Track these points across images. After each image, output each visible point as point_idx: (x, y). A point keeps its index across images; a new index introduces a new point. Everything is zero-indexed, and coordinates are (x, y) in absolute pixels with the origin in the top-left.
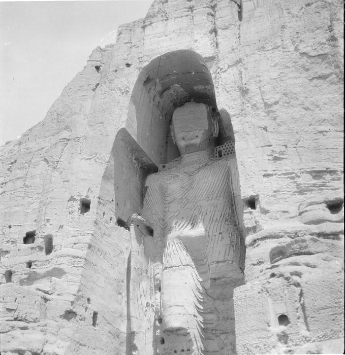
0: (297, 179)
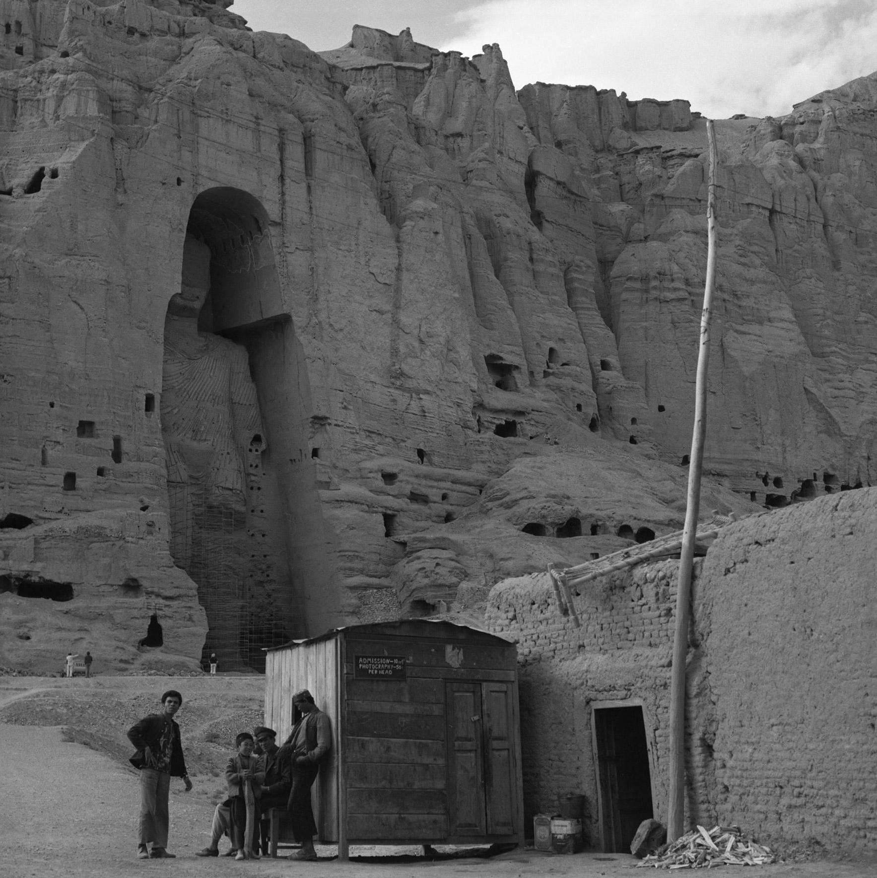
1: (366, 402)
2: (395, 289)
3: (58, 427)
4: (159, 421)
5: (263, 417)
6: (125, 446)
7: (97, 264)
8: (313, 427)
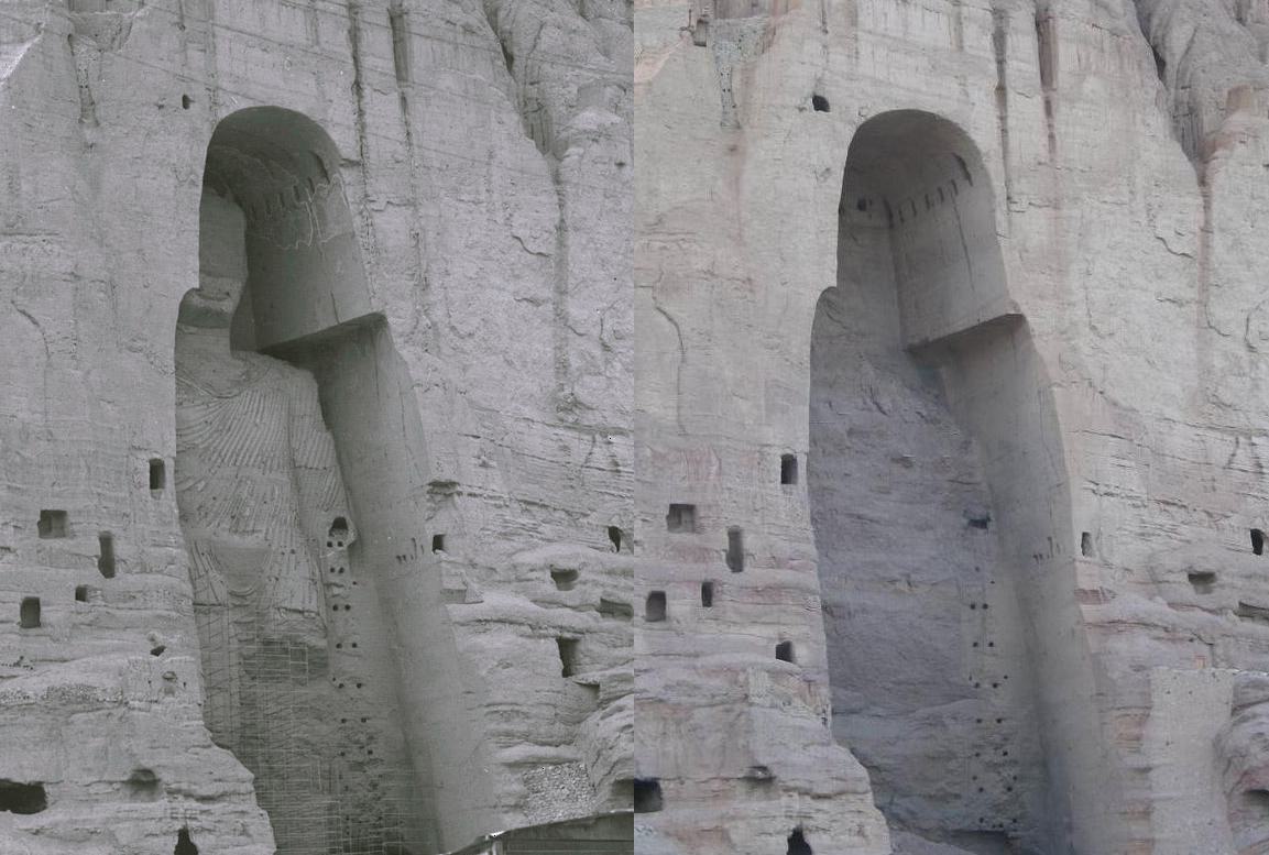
0: (1143, 511)
1: (517, 454)
2: (556, 262)
3: (6, 524)
4: (174, 504)
5: (349, 489)
6: (749, 542)
7: (57, 248)
8: (432, 499)
